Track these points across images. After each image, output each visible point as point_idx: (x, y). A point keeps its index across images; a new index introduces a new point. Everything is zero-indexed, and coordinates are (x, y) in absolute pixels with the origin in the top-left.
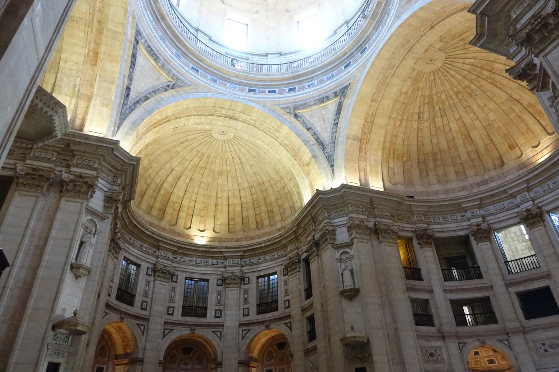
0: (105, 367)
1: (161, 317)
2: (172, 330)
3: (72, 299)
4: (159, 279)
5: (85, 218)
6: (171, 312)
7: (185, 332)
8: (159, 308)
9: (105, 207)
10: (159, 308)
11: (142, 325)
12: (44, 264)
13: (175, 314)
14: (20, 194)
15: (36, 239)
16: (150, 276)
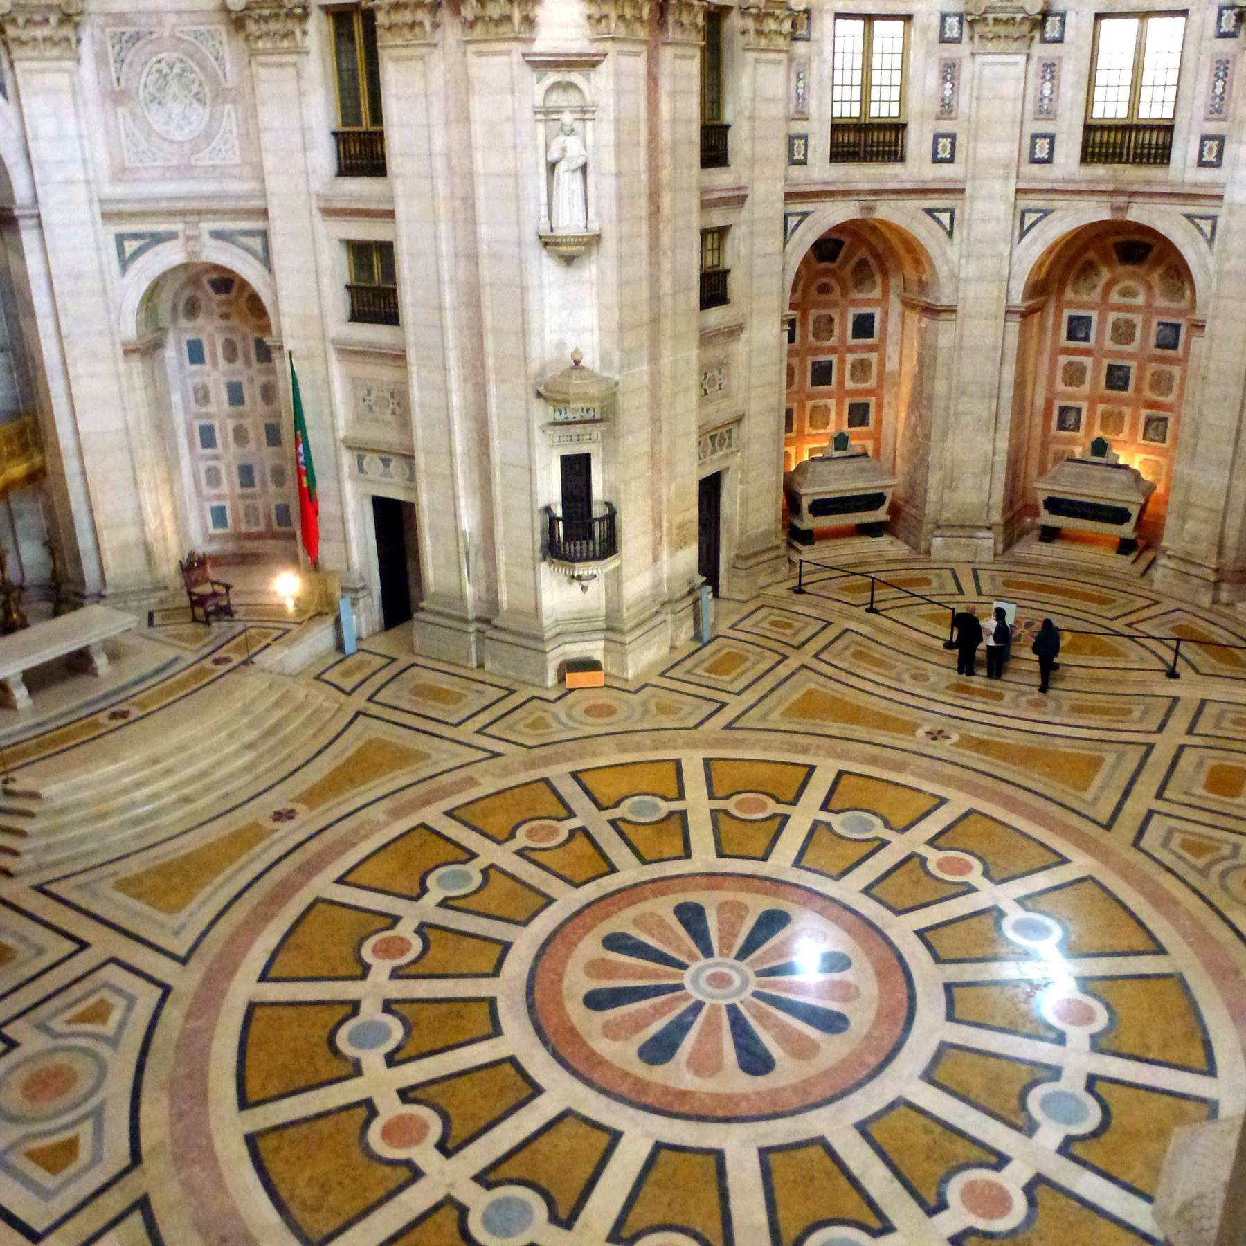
0: (878, 313)
1: (1006, 178)
2: (1046, 213)
3: (571, 318)
4: (990, 46)
5: (536, 88)
6: (1041, 153)
7: (1096, 212)
8: (992, 151)
9: (589, 17)
10: (992, 151)
11: (945, 210)
12: (484, 248)
13: (1058, 157)
14: (397, 60)
15: (457, 180)
16: (958, 41)
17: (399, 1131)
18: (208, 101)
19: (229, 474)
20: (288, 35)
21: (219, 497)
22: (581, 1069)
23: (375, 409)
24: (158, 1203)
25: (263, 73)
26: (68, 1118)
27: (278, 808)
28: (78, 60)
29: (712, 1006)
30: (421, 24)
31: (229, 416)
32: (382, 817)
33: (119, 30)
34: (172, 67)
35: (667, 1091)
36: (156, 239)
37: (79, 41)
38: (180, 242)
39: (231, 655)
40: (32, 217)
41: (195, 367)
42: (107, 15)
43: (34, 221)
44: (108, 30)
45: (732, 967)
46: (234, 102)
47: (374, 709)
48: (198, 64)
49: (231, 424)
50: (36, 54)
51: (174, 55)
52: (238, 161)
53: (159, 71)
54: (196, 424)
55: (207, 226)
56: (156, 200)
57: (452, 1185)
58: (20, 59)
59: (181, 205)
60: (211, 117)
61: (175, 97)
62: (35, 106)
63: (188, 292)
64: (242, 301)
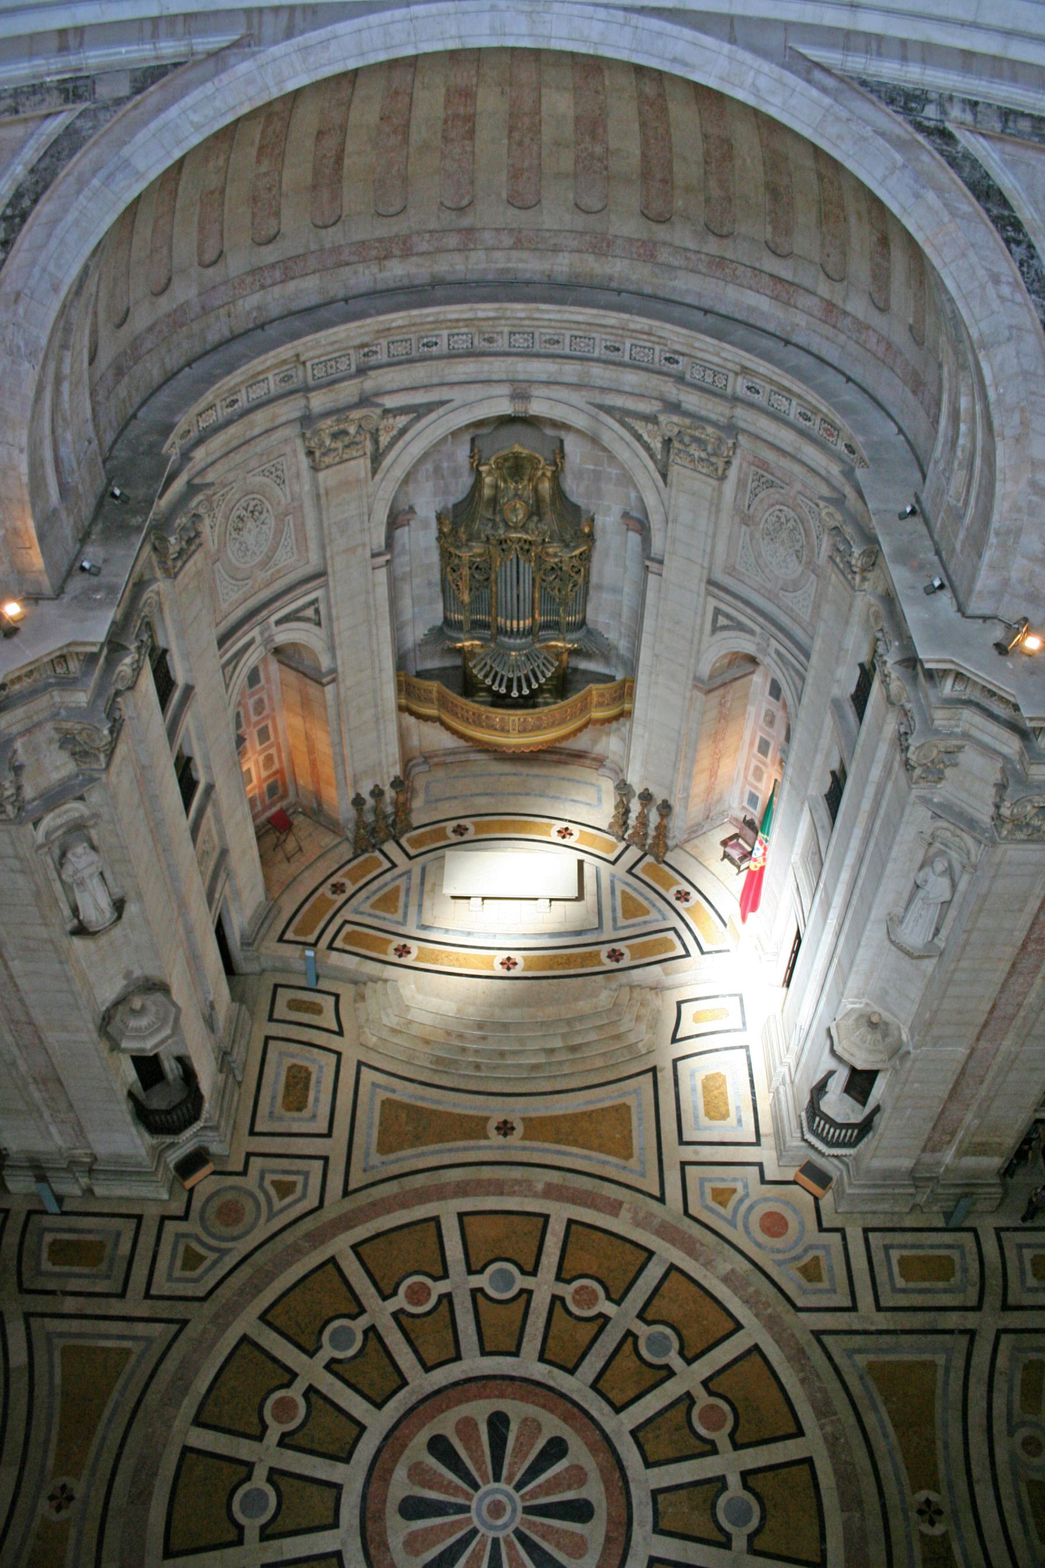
17: (285, 1408)
22: (375, 1473)
24: (190, 1331)
29: (470, 1518)
32: (540, 1187)
34: (788, 521)
35: (383, 1533)
36: (740, 627)
38: (758, 639)
44: (753, 468)
45: (514, 1510)
54: (759, 734)
57: (261, 1460)
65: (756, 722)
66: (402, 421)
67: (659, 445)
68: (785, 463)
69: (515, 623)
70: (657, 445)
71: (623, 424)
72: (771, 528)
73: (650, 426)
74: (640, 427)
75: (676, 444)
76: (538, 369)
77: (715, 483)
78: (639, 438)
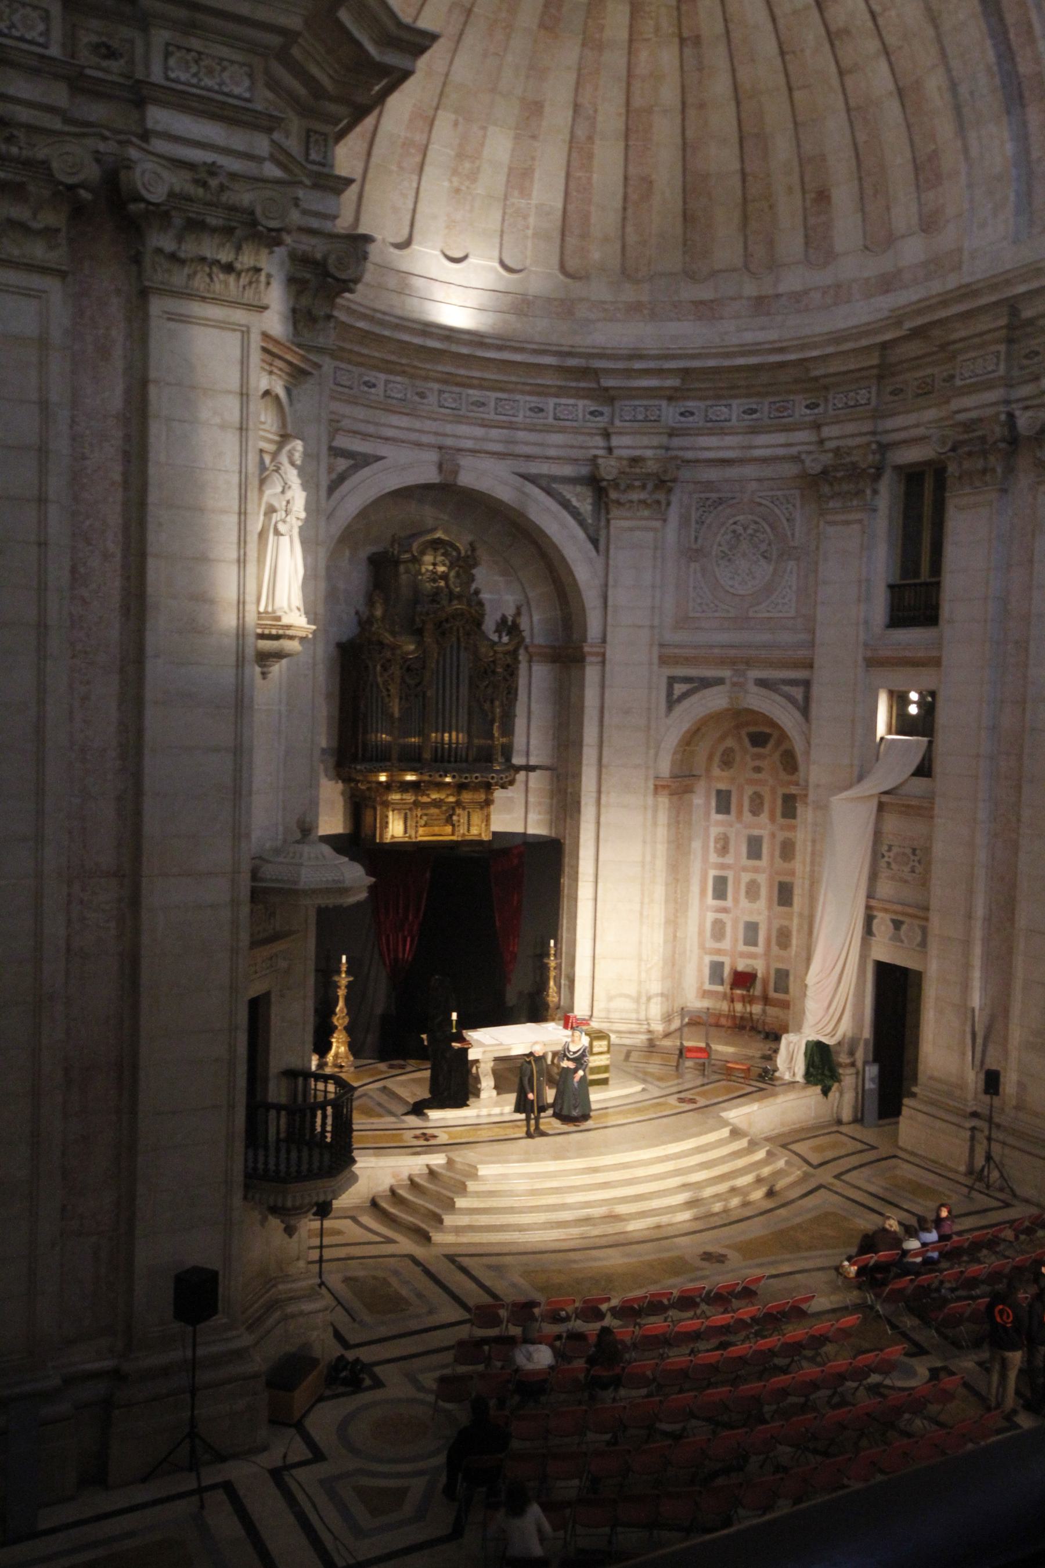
18: (774, 557)
19: (735, 928)
20: (859, 493)
21: (719, 952)
23: (893, 866)
25: (831, 530)
26: (407, 1467)
27: (709, 1249)
28: (665, 520)
30: (993, 470)
31: (745, 869)
33: (703, 495)
34: (745, 529)
36: (705, 683)
37: (668, 504)
39: (698, 1098)
40: (597, 654)
41: (720, 817)
42: (695, 483)
43: (599, 659)
44: (696, 496)
46: (798, 559)
47: (838, 1185)
48: (771, 526)
49: (746, 877)
50: (628, 515)
51: (750, 517)
52: (792, 613)
53: (734, 532)
54: (712, 873)
55: (754, 674)
56: (712, 647)
58: (617, 519)
59: (732, 652)
60: (775, 570)
61: (744, 555)
62: (619, 557)
63: (730, 743)
64: (777, 756)
65: (705, 860)
66: (342, 464)
67: (589, 508)
68: (733, 472)
69: (454, 734)
70: (586, 507)
71: (549, 492)
72: (725, 549)
73: (579, 488)
74: (569, 492)
75: (613, 495)
76: (466, 434)
77: (657, 524)
78: (566, 505)
